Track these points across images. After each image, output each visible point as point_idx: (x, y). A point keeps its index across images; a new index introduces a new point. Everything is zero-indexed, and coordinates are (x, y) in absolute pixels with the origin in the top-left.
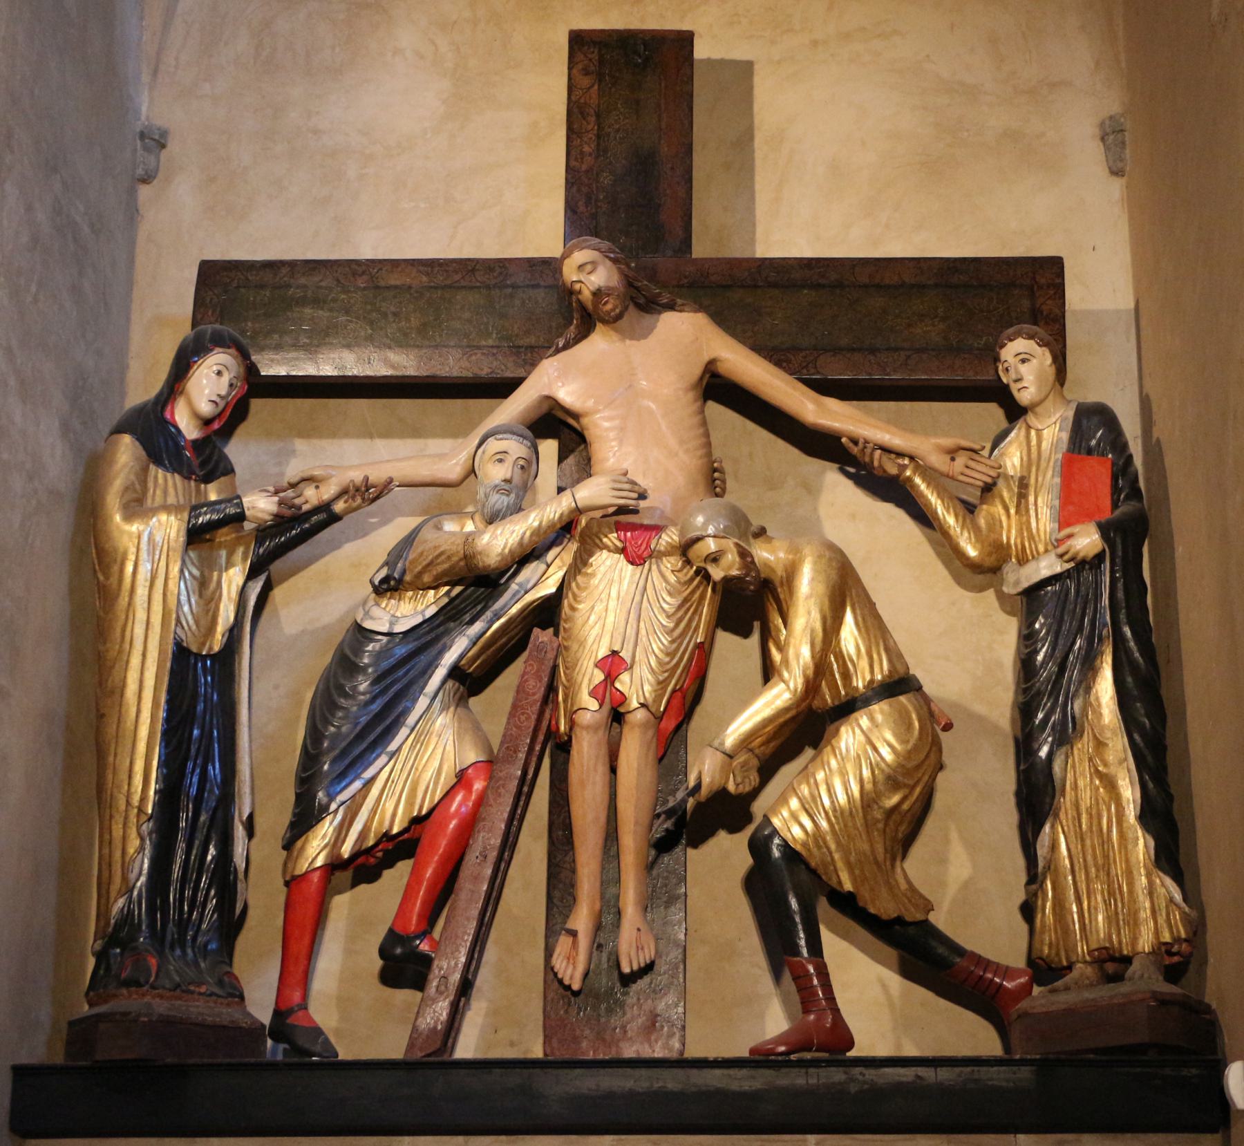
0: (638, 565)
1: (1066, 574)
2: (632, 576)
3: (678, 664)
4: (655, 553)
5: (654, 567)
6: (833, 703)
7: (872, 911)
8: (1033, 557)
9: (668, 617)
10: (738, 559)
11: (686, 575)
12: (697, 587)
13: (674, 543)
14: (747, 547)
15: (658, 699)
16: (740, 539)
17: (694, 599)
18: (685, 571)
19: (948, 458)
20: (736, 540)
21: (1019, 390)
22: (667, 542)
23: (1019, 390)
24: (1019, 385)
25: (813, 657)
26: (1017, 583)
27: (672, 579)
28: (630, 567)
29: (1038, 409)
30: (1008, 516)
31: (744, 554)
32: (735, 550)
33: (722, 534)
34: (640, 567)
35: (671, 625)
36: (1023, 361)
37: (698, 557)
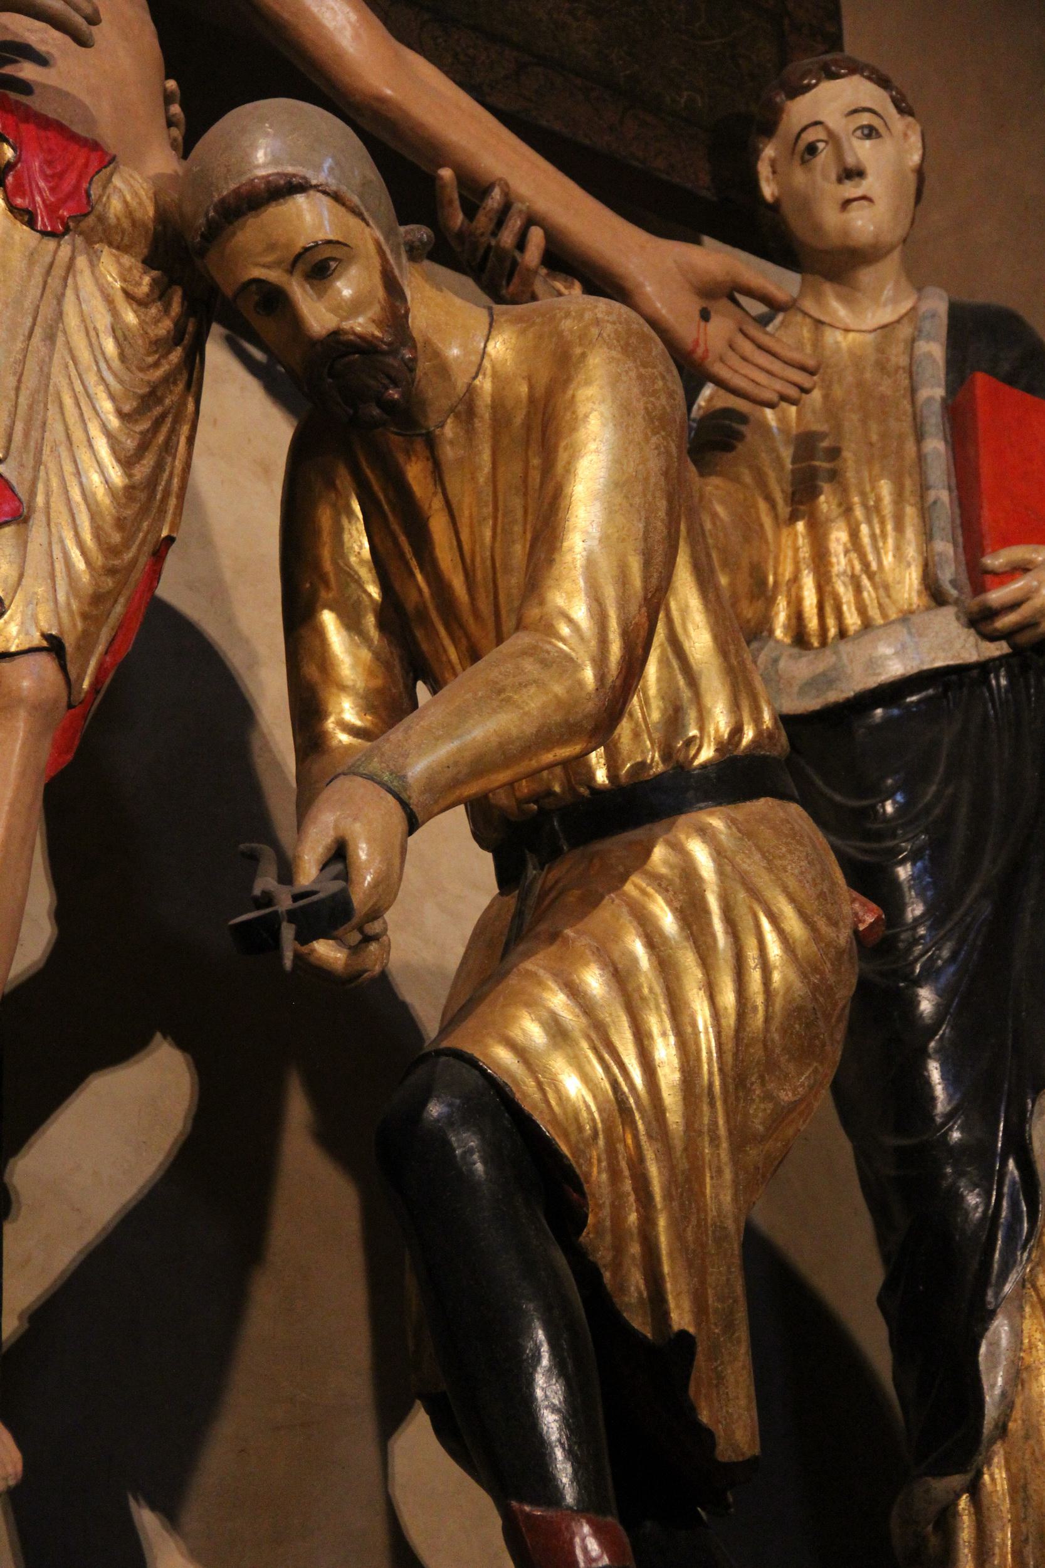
0: (44, 233)
1: (975, 673)
2: (32, 257)
3: (134, 561)
4: (91, 220)
5: (82, 262)
6: (612, 774)
7: (704, 1417)
8: (824, 643)
9: (120, 413)
10: (381, 293)
11: (156, 321)
12: (168, 380)
13: (138, 215)
14: (397, 272)
15: (86, 640)
16: (387, 239)
17: (167, 402)
18: (153, 311)
19: (693, 305)
20: (382, 239)
21: (846, 204)
22: (126, 202)
23: (846, 204)
24: (851, 190)
25: (645, 589)
26: (824, 680)
27: (130, 318)
28: (22, 232)
29: (866, 276)
30: (776, 517)
31: (392, 287)
32: (376, 261)
33: (356, 200)
34: (51, 244)
35: (130, 444)
36: (870, 133)
37: (272, 247)
